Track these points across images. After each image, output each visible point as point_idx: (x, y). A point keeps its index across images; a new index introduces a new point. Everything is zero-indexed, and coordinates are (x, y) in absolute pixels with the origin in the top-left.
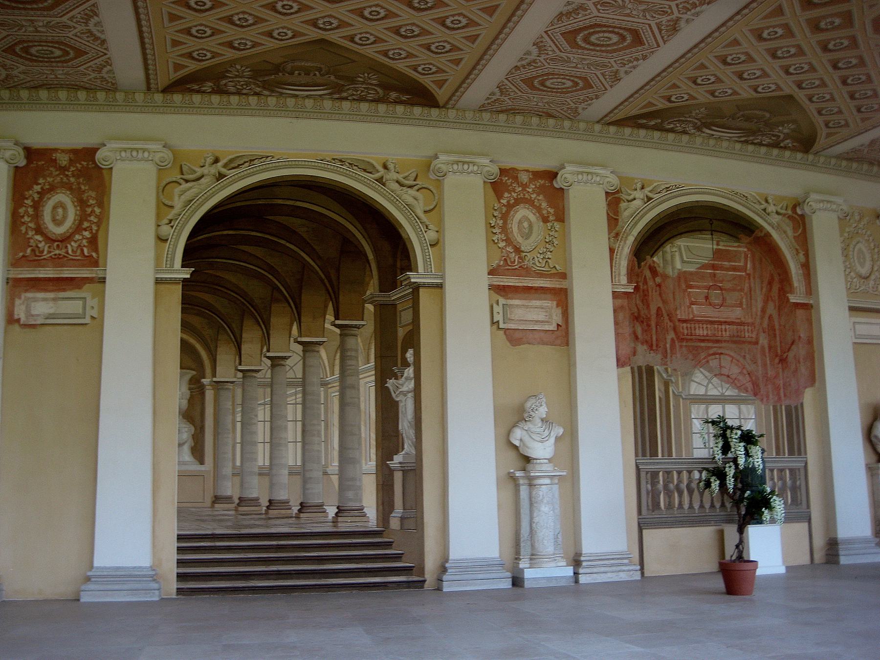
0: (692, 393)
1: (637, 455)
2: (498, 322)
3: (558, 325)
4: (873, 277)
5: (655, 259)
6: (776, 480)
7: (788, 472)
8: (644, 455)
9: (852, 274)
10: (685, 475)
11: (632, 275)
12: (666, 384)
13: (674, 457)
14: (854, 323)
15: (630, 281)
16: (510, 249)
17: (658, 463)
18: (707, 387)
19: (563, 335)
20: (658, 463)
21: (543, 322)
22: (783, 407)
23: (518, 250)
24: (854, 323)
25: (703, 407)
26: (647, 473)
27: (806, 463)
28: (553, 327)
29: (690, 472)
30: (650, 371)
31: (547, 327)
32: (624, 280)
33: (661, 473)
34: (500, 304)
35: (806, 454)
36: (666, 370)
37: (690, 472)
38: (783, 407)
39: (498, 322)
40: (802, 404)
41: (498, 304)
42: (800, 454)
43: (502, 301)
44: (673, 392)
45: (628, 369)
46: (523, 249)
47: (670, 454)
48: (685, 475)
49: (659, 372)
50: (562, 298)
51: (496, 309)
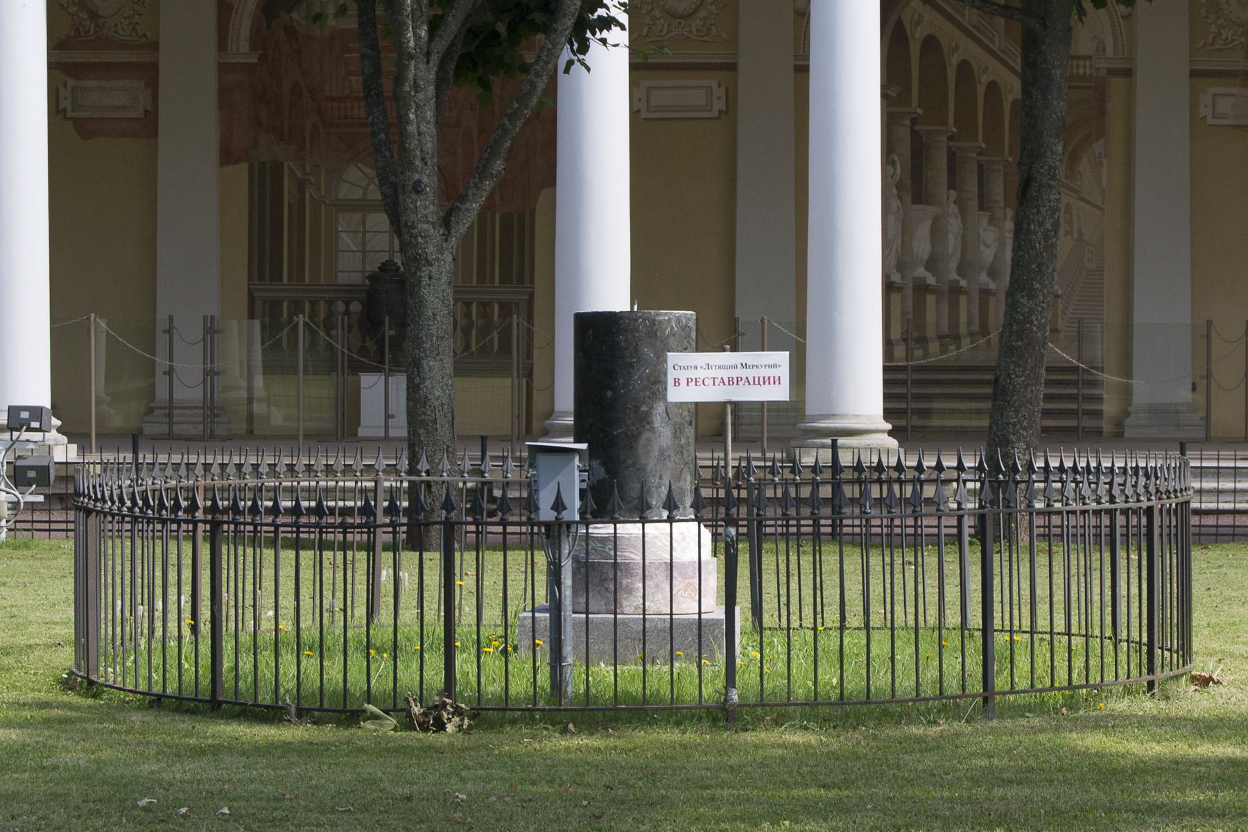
0: (341, 196)
1: (250, 278)
2: (65, 110)
3: (146, 111)
4: (702, 13)
5: (294, 15)
6: (474, 318)
7: (496, 307)
8: (261, 278)
9: (657, 13)
10: (322, 307)
11: (257, 39)
12: (301, 186)
13: (307, 281)
14: (648, 88)
15: (253, 47)
16: (84, 15)
17: (281, 290)
18: (365, 189)
19: (148, 126)
20: (281, 290)
21: (124, 107)
22: (498, 216)
23: (94, 16)
24: (648, 88)
25: (358, 216)
26: (264, 302)
27: (532, 295)
28: (139, 114)
29: (330, 303)
30: (277, 168)
31: (131, 115)
32: (244, 46)
33: (285, 304)
34: (69, 88)
35: (532, 281)
36: (304, 169)
37: (330, 303)
38: (498, 216)
39: (65, 110)
40: (533, 212)
41: (65, 85)
42: (521, 280)
43: (71, 82)
44: (311, 196)
45: (244, 167)
46: (101, 13)
47: (301, 277)
48: (322, 307)
49: (290, 168)
50: (150, 73)
51: (62, 91)
